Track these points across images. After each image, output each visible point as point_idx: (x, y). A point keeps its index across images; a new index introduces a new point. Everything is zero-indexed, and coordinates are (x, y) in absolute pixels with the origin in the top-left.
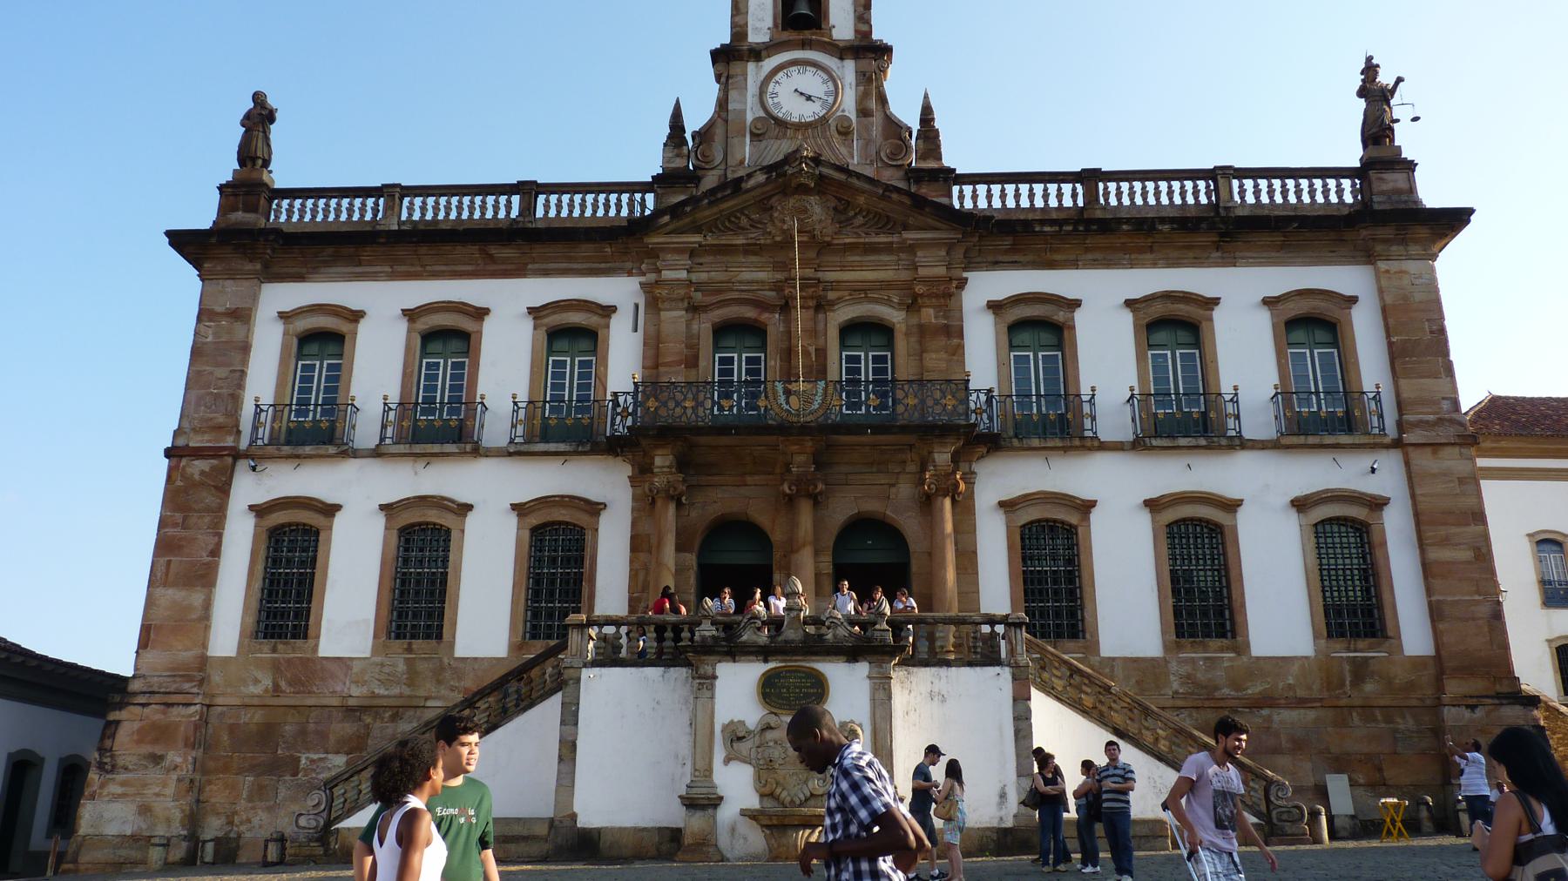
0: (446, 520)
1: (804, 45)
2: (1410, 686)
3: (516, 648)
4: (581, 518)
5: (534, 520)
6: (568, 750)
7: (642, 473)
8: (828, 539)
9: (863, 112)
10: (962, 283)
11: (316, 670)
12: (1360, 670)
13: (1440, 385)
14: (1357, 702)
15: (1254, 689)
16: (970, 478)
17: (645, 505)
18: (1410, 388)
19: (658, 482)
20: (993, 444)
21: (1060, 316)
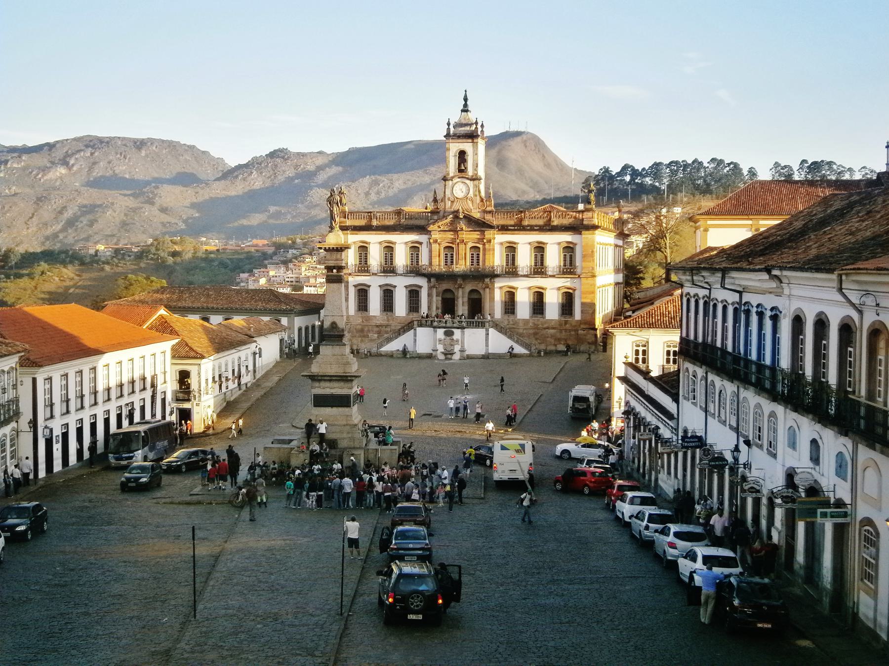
0: (392, 289)
1: (462, 177)
2: (575, 326)
3: (408, 314)
4: (418, 289)
5: (409, 289)
6: (415, 340)
7: (429, 281)
8: (467, 295)
9: (476, 196)
10: (494, 238)
11: (369, 318)
12: (566, 322)
13: (590, 264)
14: (564, 328)
15: (545, 326)
16: (493, 283)
17: (430, 288)
18: (584, 264)
19: (432, 284)
20: (497, 276)
21: (515, 246)
